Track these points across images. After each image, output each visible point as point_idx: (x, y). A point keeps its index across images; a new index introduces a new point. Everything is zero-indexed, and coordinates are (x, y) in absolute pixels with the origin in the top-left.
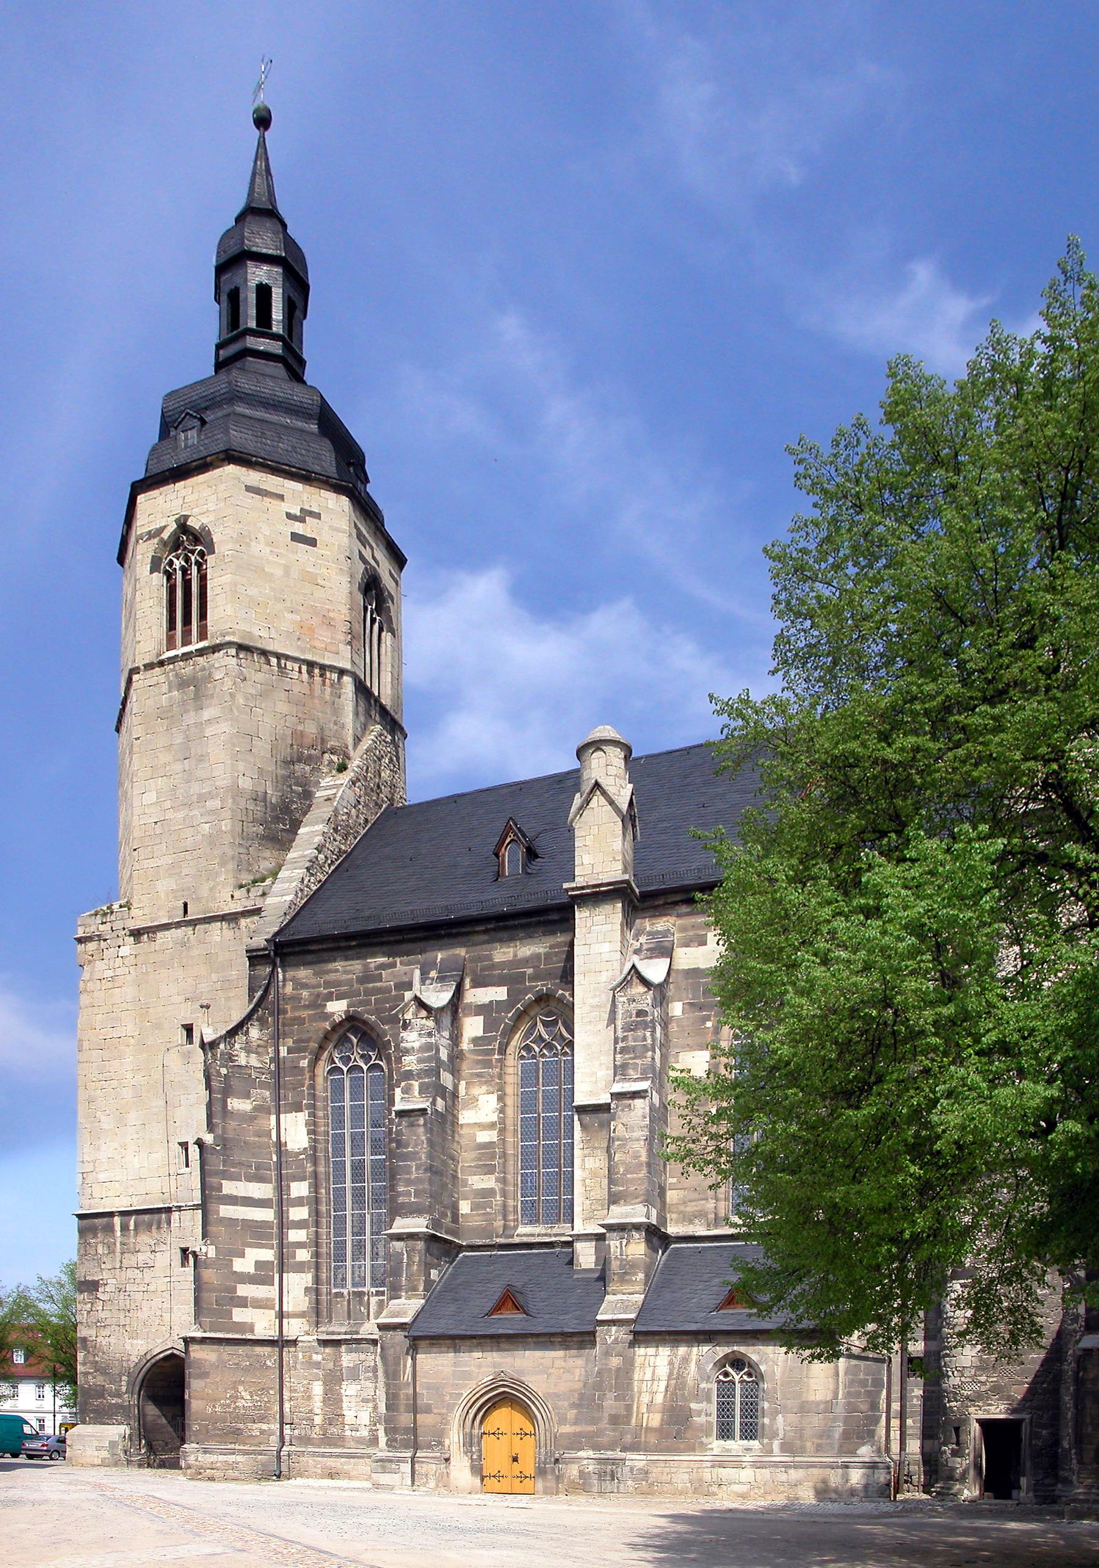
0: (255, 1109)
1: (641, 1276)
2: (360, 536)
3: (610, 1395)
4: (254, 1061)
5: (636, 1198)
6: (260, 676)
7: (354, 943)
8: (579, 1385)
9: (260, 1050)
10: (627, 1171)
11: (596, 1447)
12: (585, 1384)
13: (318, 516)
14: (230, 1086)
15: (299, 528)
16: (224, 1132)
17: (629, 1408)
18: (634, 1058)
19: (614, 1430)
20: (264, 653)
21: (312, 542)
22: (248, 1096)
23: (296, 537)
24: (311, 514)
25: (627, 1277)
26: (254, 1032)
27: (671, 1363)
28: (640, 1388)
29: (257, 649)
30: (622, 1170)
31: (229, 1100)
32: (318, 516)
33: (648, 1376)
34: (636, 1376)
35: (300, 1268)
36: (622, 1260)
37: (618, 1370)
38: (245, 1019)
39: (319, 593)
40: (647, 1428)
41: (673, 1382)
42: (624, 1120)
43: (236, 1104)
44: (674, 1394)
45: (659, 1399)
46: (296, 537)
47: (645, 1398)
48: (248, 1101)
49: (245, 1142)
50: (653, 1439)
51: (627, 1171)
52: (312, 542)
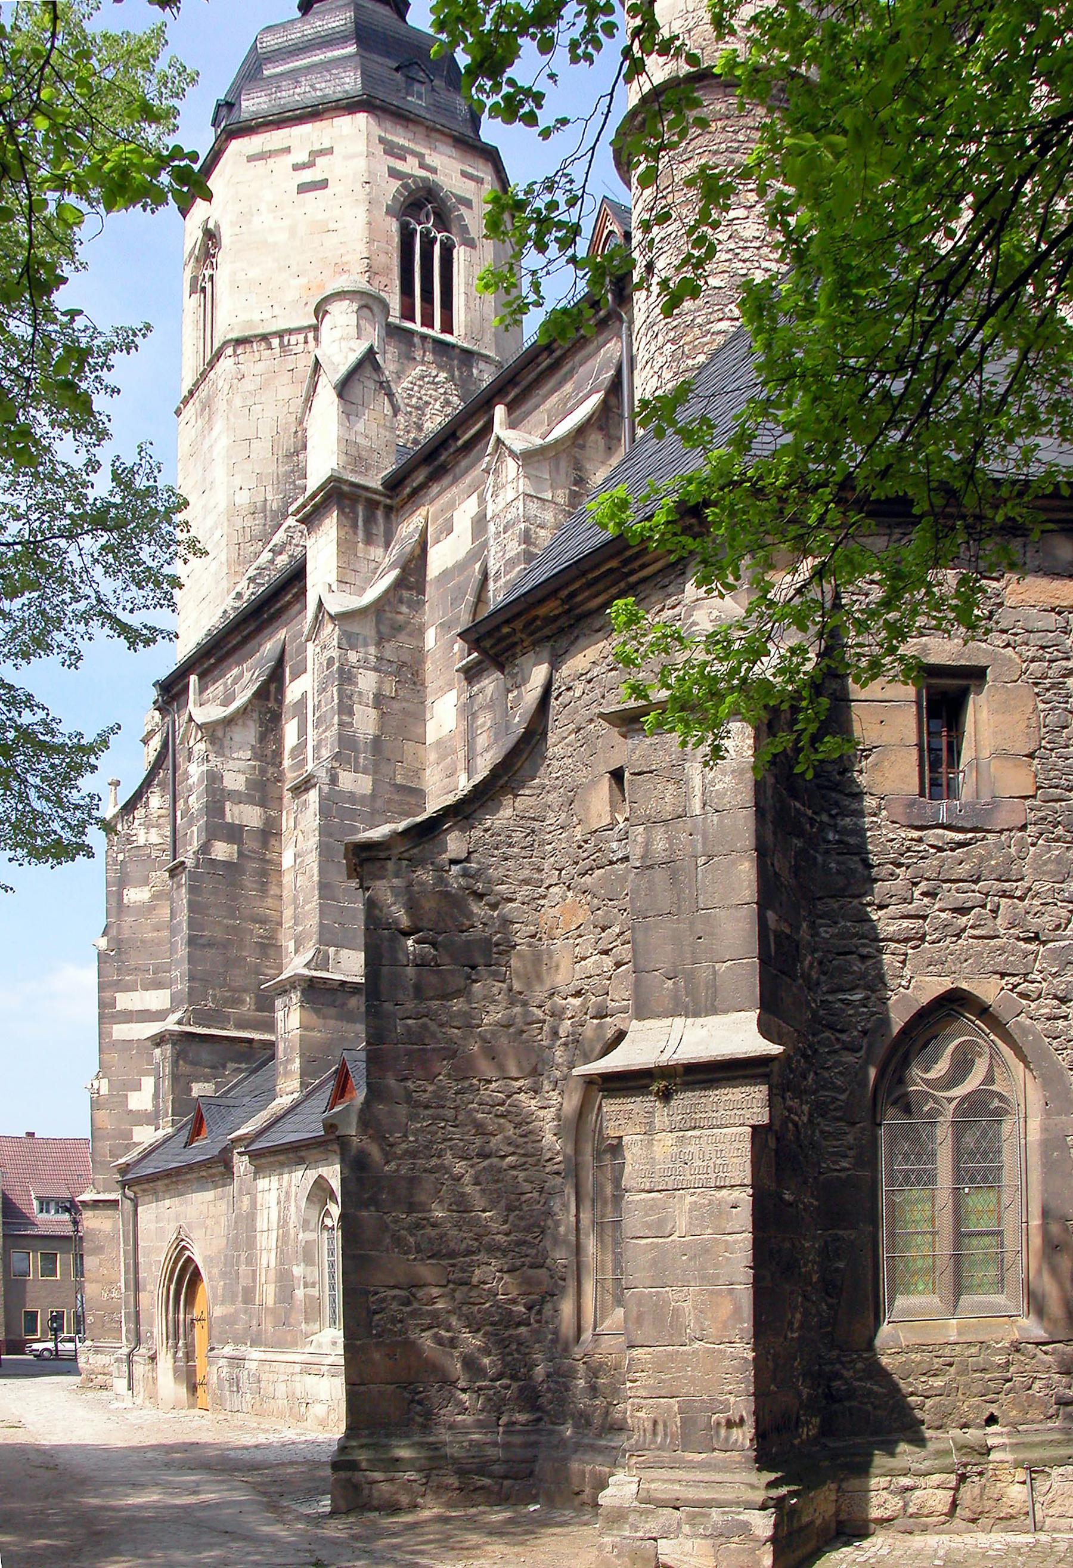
0: (154, 897)
2: (392, 150)
4: (154, 837)
6: (260, 367)
7: (212, 661)
9: (161, 821)
13: (330, 151)
14: (127, 874)
15: (307, 176)
16: (119, 933)
20: (264, 338)
21: (323, 185)
22: (145, 882)
23: (303, 188)
24: (322, 153)
26: (156, 801)
29: (256, 336)
31: (125, 892)
32: (330, 151)
38: (141, 787)
39: (331, 240)
43: (135, 895)
46: (303, 188)
48: (147, 888)
49: (142, 941)
52: (323, 185)
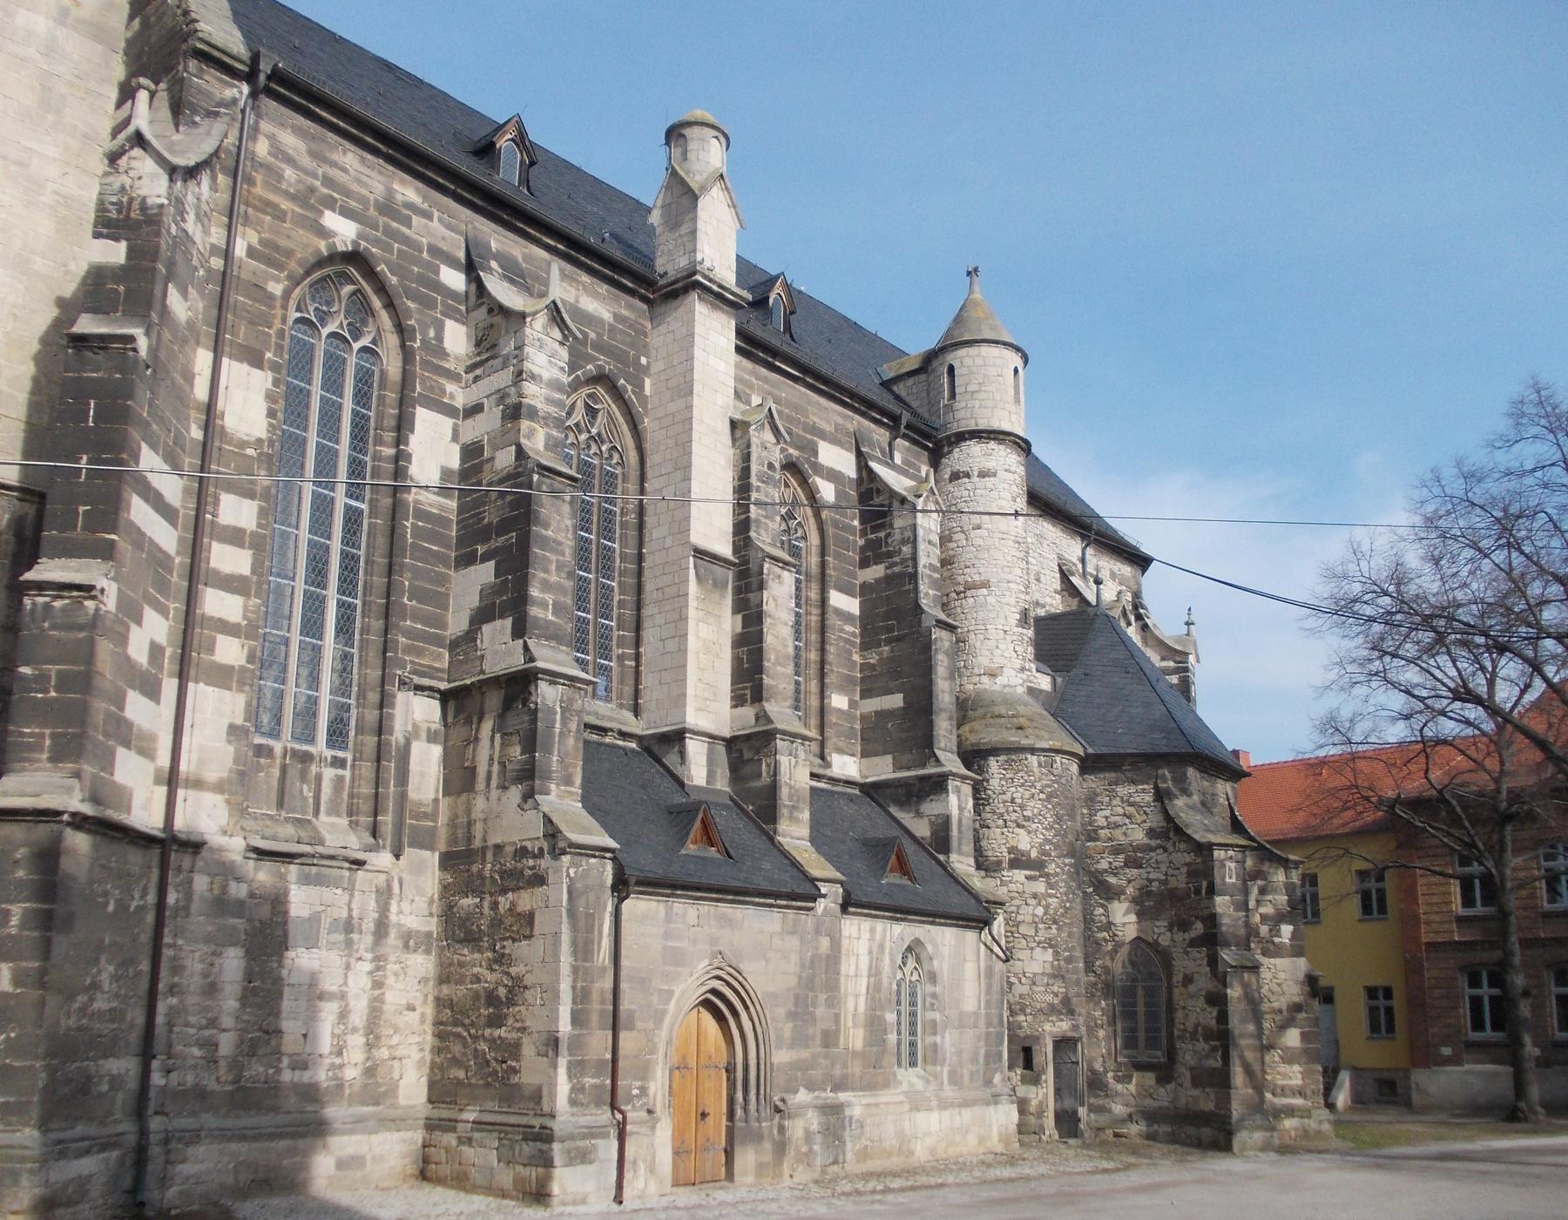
1: (806, 815)
3: (822, 997)
5: (785, 700)
8: (793, 981)
10: (777, 662)
11: (811, 1087)
12: (800, 977)
17: (837, 1017)
18: (766, 517)
19: (826, 1056)
25: (796, 814)
27: (870, 952)
28: (846, 989)
30: (773, 658)
33: (852, 973)
34: (843, 971)
35: (222, 676)
36: (791, 787)
37: (828, 957)
40: (854, 1053)
41: (872, 979)
42: (775, 592)
44: (873, 999)
45: (862, 1007)
47: (850, 1006)
50: (856, 1069)
51: (777, 662)
